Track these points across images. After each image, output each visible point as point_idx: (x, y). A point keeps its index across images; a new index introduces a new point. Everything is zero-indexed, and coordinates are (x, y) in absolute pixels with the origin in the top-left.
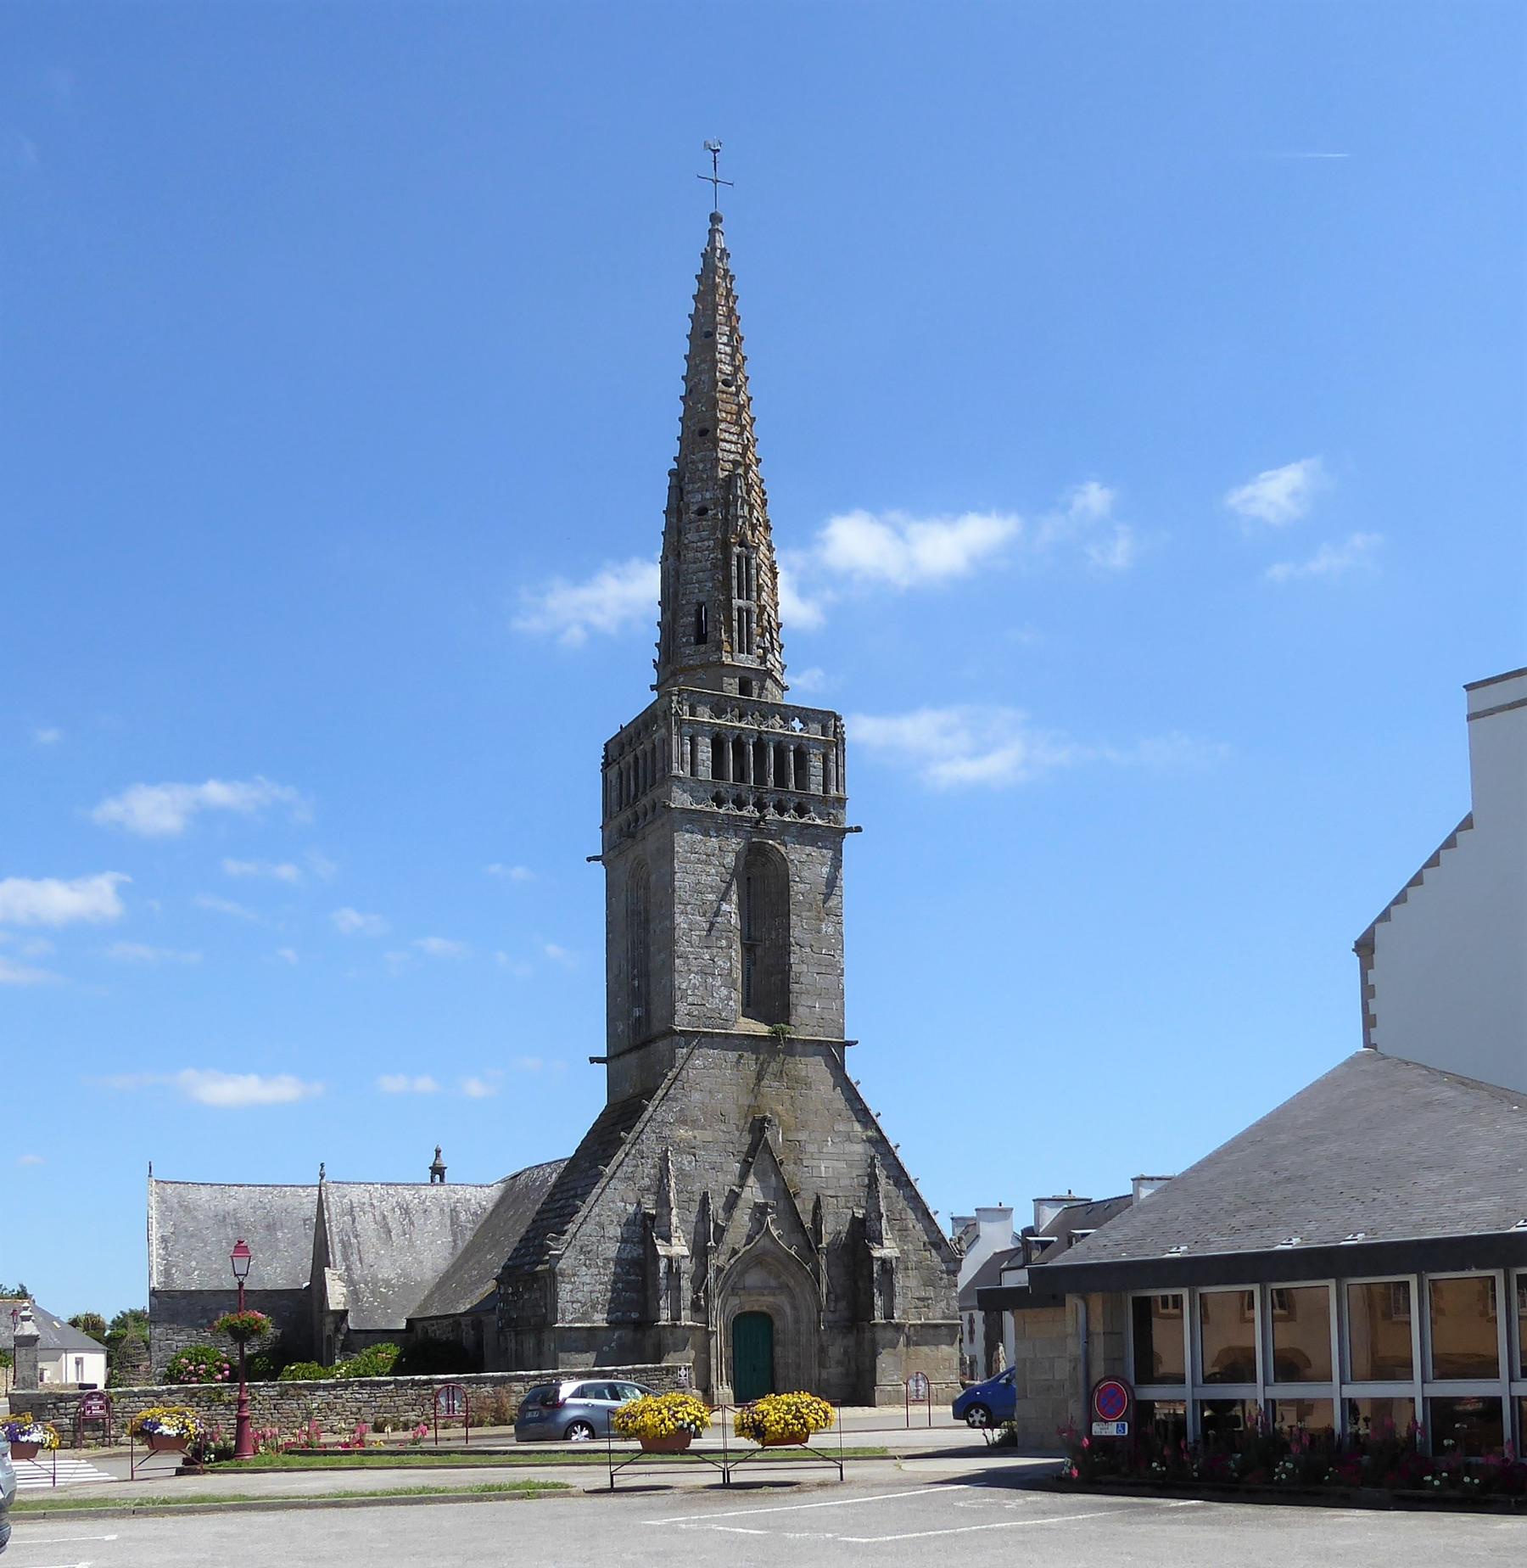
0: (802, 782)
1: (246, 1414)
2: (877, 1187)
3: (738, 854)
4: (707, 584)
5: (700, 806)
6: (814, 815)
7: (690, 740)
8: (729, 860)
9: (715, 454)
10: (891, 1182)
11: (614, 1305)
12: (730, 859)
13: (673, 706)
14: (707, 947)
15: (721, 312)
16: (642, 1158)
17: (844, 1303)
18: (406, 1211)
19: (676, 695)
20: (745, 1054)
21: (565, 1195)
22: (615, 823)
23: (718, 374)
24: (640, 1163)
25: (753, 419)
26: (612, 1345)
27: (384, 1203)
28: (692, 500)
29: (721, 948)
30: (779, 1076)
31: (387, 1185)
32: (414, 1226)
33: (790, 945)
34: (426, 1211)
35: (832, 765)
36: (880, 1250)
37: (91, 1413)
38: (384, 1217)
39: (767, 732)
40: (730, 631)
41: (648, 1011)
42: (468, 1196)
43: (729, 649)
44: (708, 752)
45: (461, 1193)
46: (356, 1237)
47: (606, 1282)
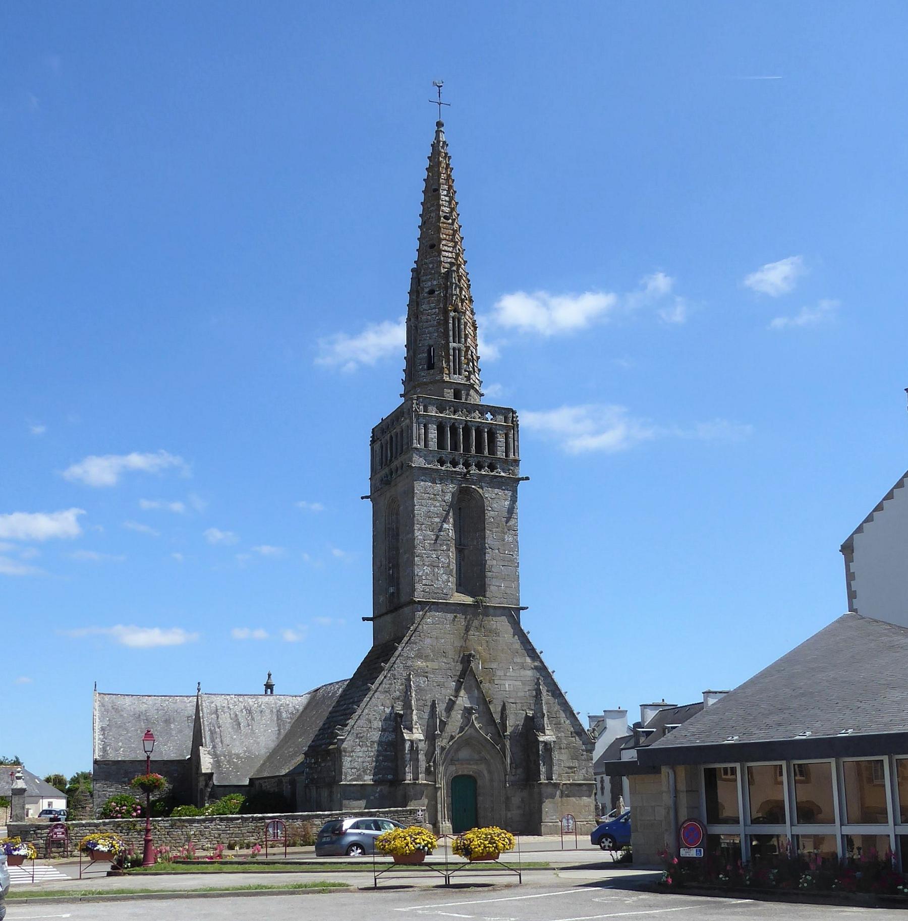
0: (492, 451)
1: (150, 838)
2: (541, 697)
4: (434, 334)
5: (430, 465)
6: (500, 470)
7: (424, 426)
8: (447, 498)
9: (439, 259)
10: (550, 694)
11: (377, 771)
12: (448, 497)
13: (414, 406)
14: (434, 550)
15: (442, 177)
16: (395, 679)
17: (521, 769)
18: (250, 712)
19: (415, 400)
20: (458, 615)
21: (347, 702)
22: (378, 476)
23: (441, 213)
24: (393, 682)
25: (462, 238)
26: (376, 796)
27: (236, 706)
28: (425, 286)
29: (443, 551)
30: (477, 629)
31: (238, 695)
32: (254, 721)
33: (486, 548)
34: (261, 712)
35: (511, 441)
36: (543, 737)
37: (57, 837)
38: (236, 715)
39: (471, 421)
40: (448, 362)
41: (398, 589)
42: (288, 702)
43: (447, 372)
44: (435, 433)
45: (284, 700)
46: (219, 727)
47: (372, 756)
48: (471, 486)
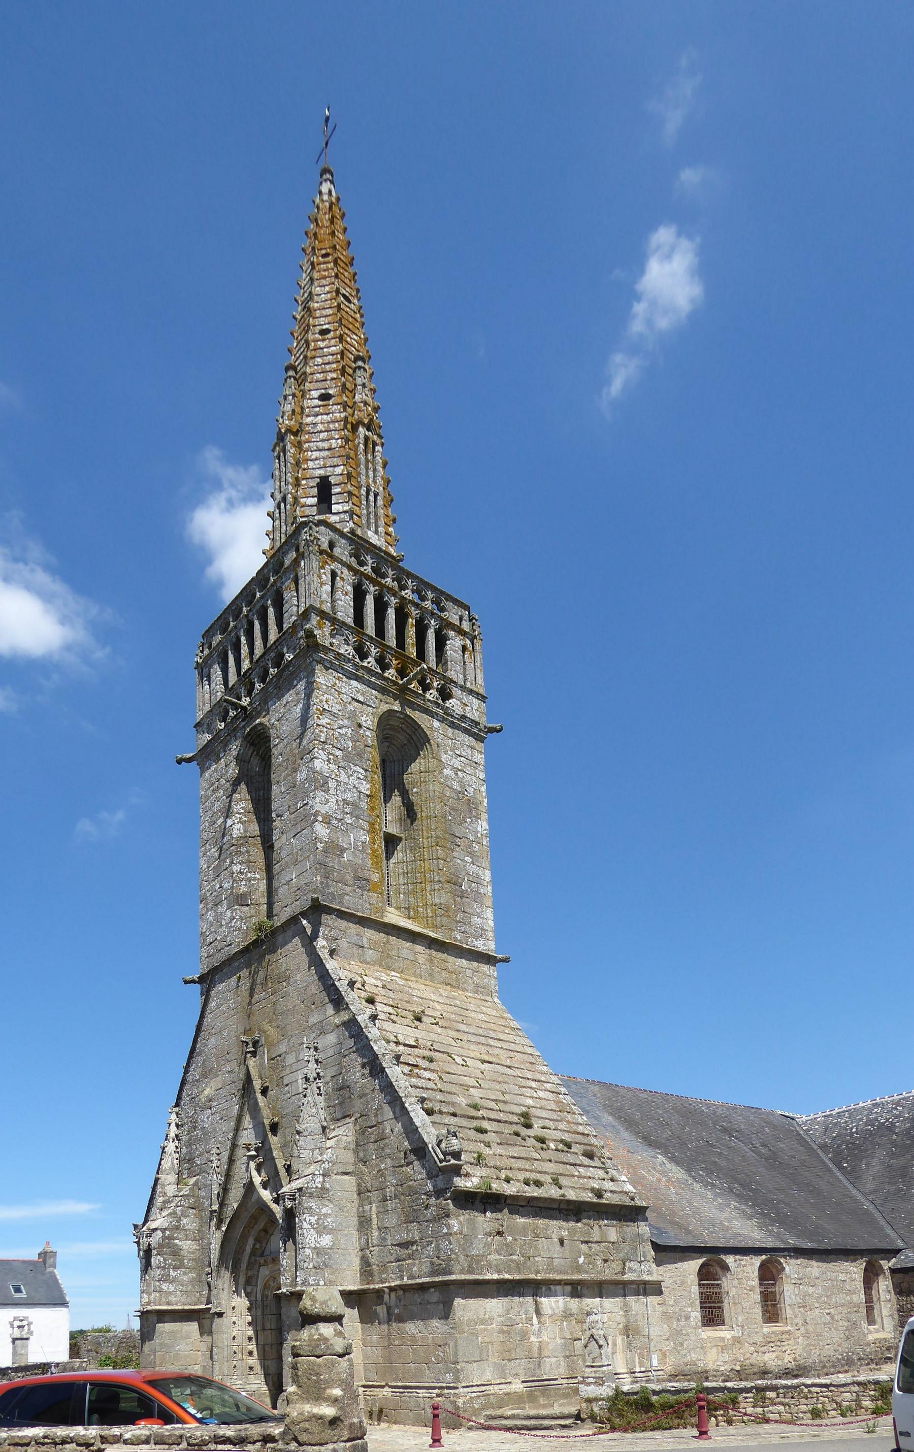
3: (239, 759)
48: (254, 724)
